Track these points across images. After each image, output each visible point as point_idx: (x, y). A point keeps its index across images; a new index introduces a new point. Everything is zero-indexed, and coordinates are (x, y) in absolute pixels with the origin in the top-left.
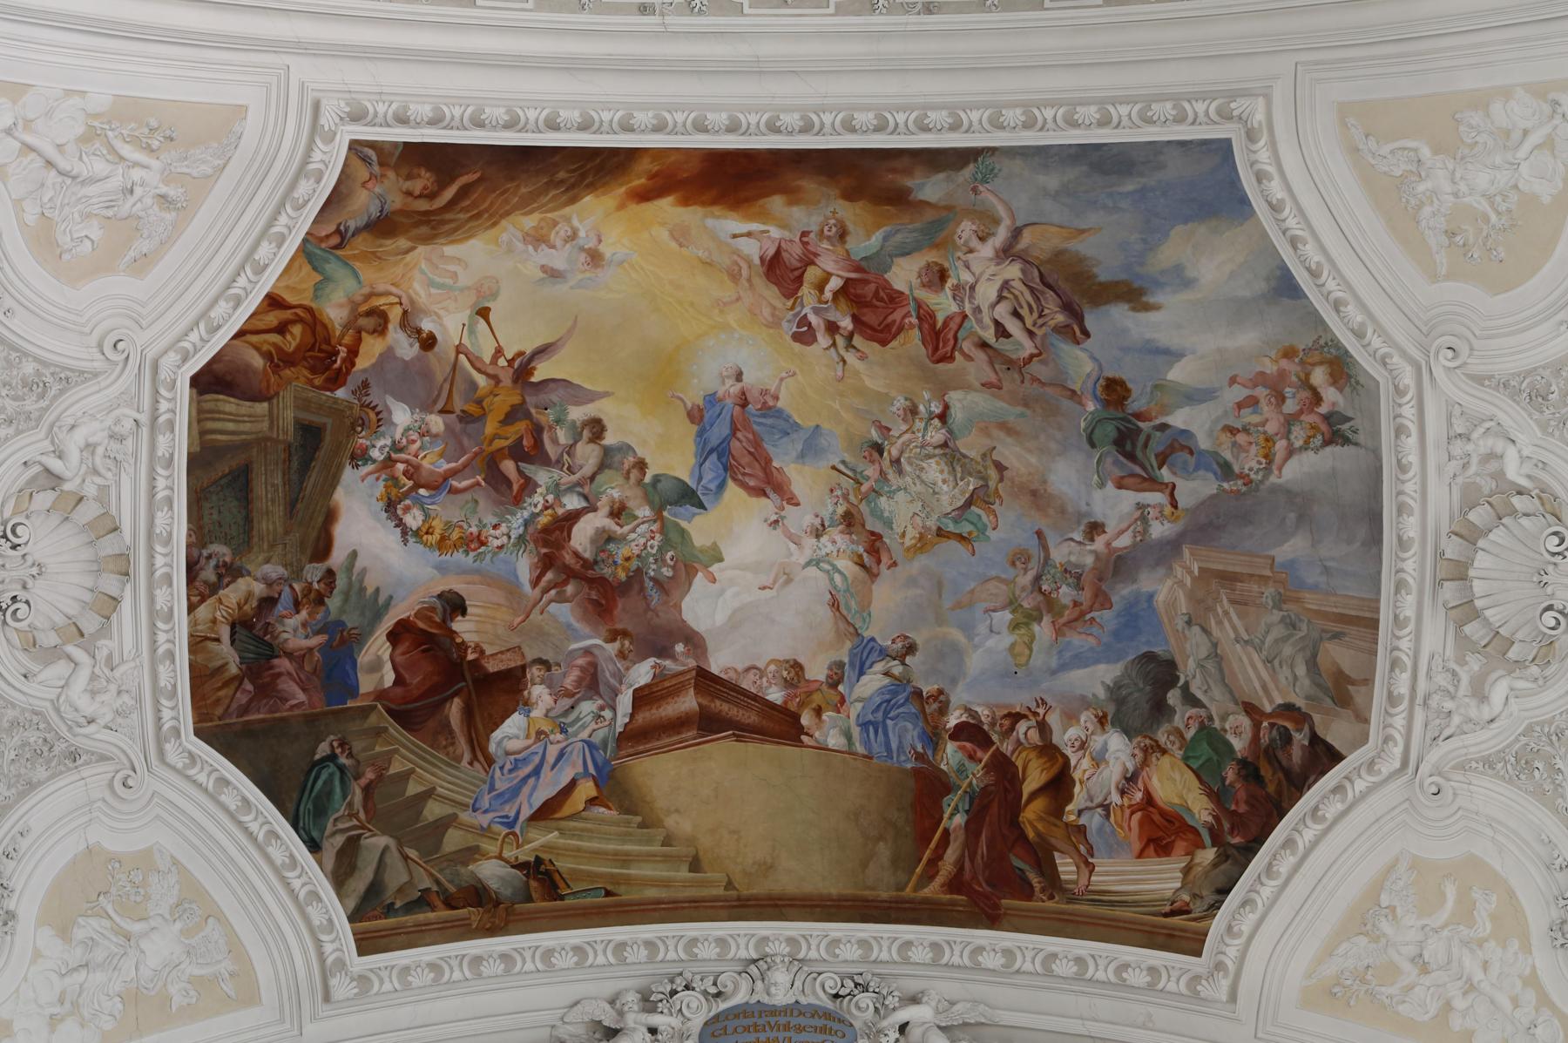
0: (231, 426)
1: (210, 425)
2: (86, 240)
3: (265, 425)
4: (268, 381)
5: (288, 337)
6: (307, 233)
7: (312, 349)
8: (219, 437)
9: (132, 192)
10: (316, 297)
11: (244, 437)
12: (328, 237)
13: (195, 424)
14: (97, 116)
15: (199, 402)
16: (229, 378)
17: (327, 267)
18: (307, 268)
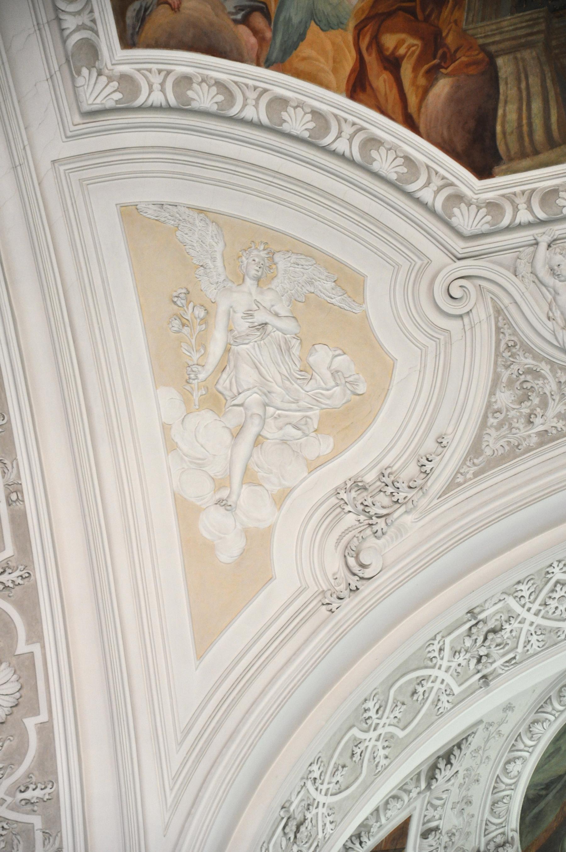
0: (537, 106)
1: (539, 135)
2: (333, 367)
3: (527, 54)
4: (468, 65)
5: (402, 51)
6: (258, 64)
7: (412, 12)
8: (554, 118)
9: (264, 325)
10: (340, 25)
11: (549, 83)
12: (255, 32)
13: (542, 157)
14: (187, 402)
15: (511, 159)
16: (471, 124)
17: (296, 20)
18: (304, 50)
